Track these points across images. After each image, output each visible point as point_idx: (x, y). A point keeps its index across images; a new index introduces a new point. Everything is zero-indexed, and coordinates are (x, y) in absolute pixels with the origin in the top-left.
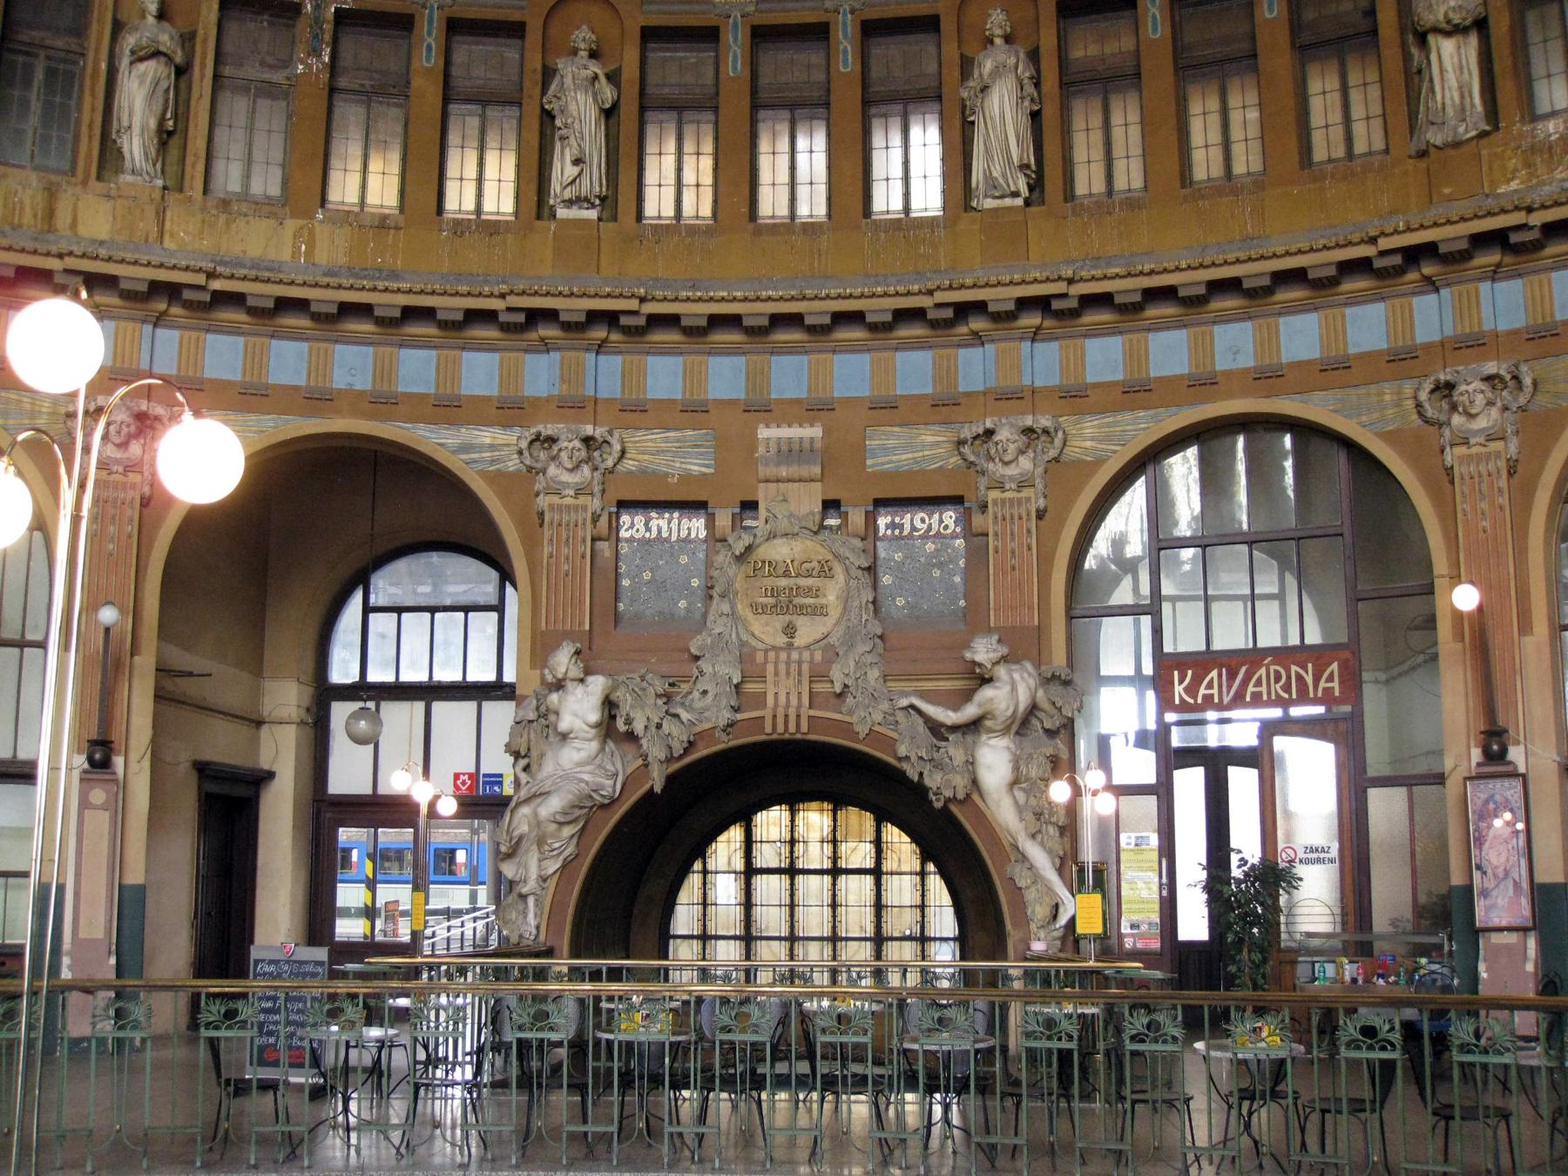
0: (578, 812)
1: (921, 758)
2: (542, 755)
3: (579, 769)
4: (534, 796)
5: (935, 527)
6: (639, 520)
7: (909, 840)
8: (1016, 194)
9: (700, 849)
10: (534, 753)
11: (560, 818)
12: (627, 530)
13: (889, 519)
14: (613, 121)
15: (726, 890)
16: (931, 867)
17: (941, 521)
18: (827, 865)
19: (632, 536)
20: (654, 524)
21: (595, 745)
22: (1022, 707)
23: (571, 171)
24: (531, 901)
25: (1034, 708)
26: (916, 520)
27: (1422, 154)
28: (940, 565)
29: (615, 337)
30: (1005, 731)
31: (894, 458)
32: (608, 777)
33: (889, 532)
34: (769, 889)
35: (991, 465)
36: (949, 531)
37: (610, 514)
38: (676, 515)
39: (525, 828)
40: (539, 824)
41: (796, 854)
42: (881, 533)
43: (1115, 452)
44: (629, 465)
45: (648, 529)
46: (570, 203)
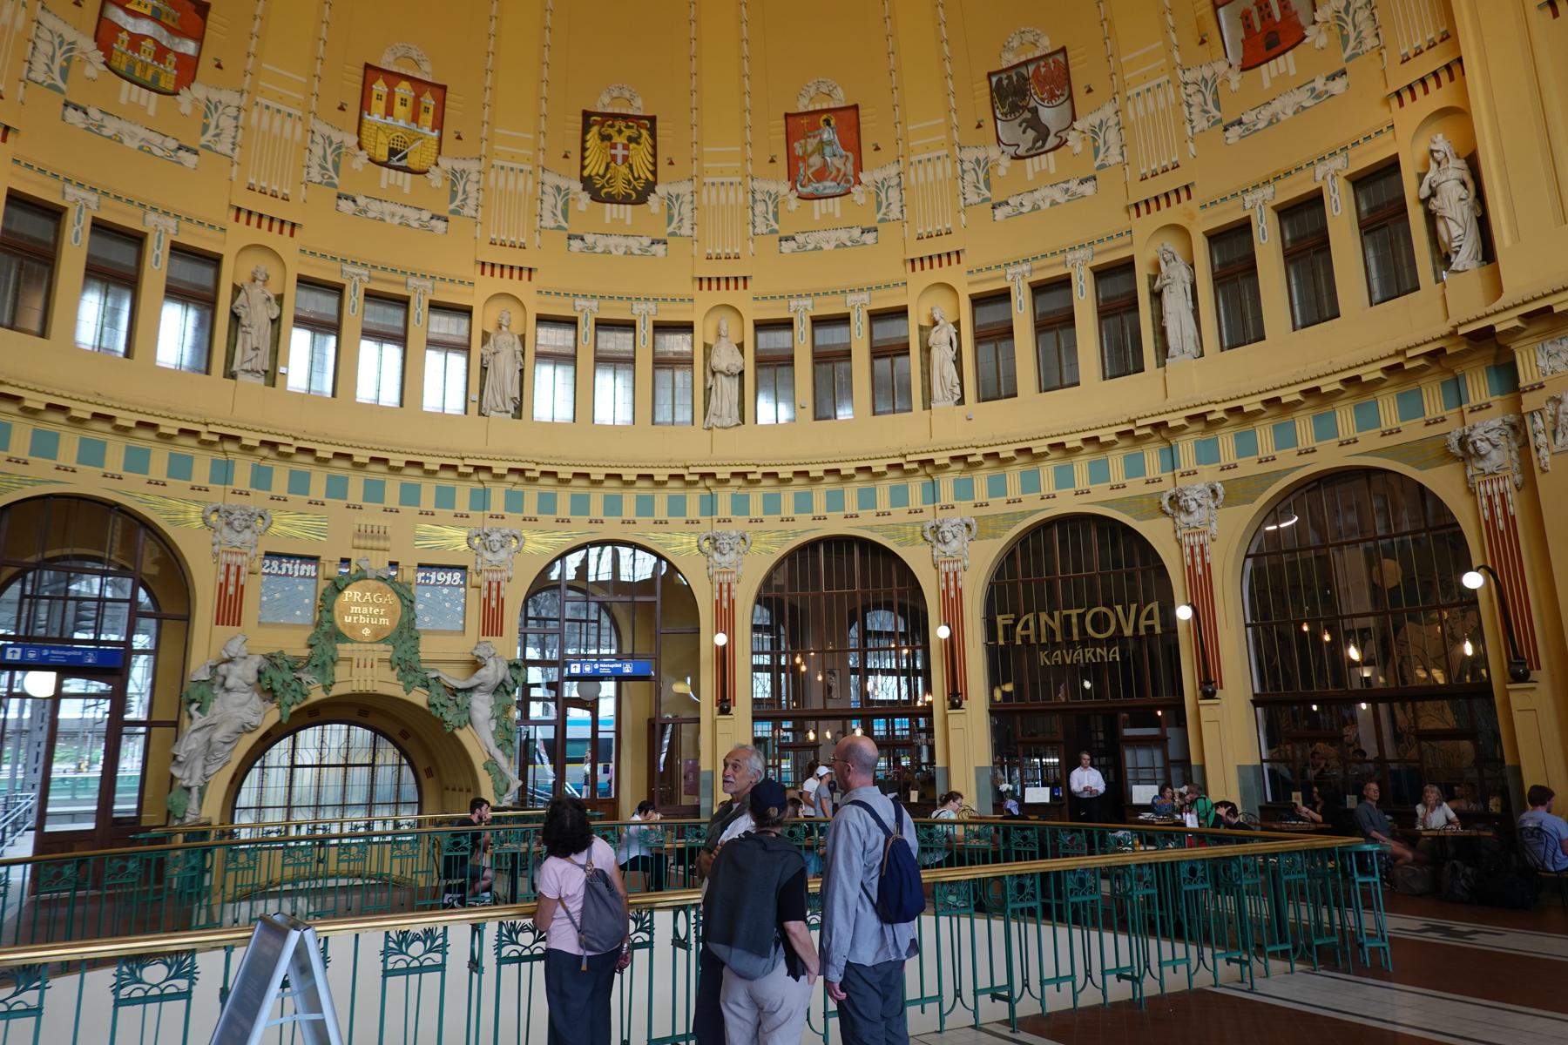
4: (205, 726)
6: (275, 563)
8: (508, 412)
14: (276, 326)
15: (277, 778)
18: (342, 762)
20: (284, 566)
22: (499, 681)
23: (251, 354)
24: (195, 791)
25: (504, 680)
26: (441, 576)
27: (709, 429)
28: (451, 602)
30: (488, 692)
34: (305, 778)
39: (193, 746)
40: (209, 742)
44: (272, 530)
46: (247, 371)
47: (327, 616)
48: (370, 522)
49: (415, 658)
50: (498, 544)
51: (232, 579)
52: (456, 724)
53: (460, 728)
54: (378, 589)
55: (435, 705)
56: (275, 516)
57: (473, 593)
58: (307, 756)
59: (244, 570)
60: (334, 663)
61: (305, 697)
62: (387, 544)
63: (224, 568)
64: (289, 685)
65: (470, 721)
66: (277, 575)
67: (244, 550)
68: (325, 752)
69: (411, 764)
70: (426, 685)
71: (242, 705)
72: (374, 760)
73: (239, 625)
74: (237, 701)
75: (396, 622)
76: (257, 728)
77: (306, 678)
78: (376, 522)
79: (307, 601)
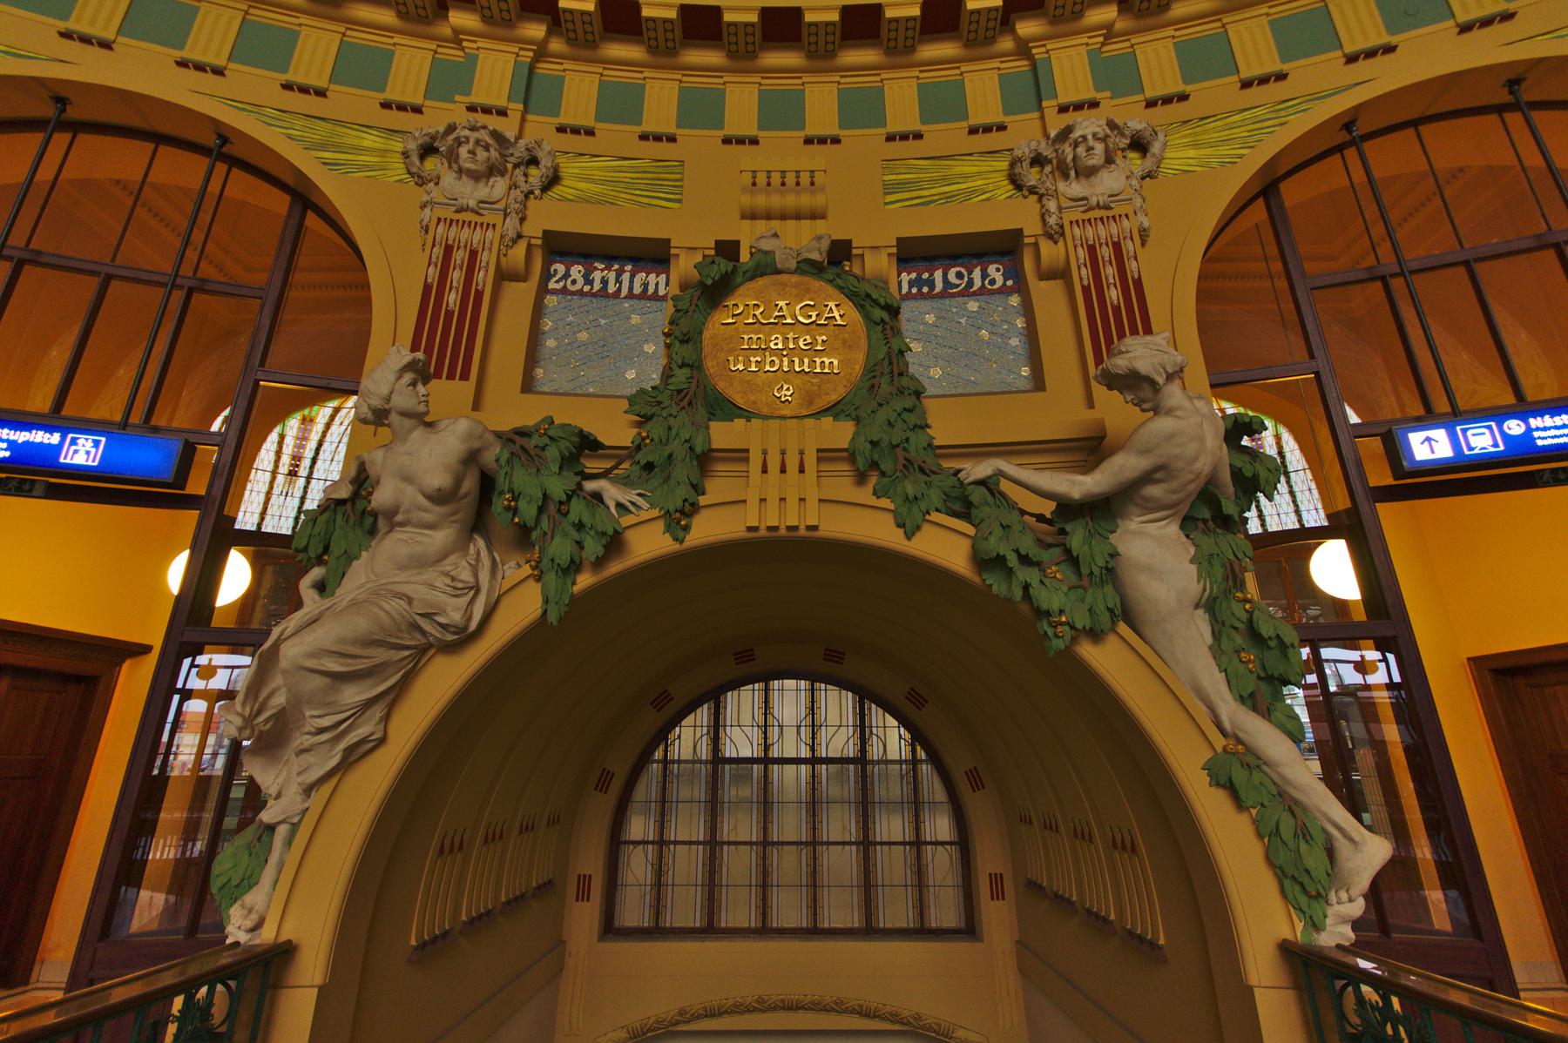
0: (382, 655)
1: (1025, 560)
2: (349, 558)
3: (402, 577)
5: (978, 283)
6: (577, 271)
7: (896, 724)
9: (662, 735)
10: (336, 550)
11: (334, 666)
12: (557, 282)
13: (914, 275)
16: (922, 754)
17: (984, 275)
19: (565, 286)
20: (597, 276)
21: (441, 537)
29: (556, 45)
31: (925, 193)
32: (457, 592)
33: (914, 290)
35: (1061, 186)
36: (999, 282)
37: (530, 246)
38: (628, 268)
41: (770, 741)
42: (905, 290)
43: (1240, 157)
45: (589, 281)
47: (683, 352)
48: (776, 164)
49: (918, 440)
50: (1099, 148)
51: (456, 276)
52: (1082, 621)
53: (1095, 635)
54: (804, 292)
55: (1000, 560)
56: (569, 168)
57: (1047, 296)
58: (741, 743)
59: (487, 258)
60: (705, 460)
61: (615, 543)
62: (819, 200)
63: (438, 251)
64: (563, 507)
65: (1126, 613)
66: (580, 293)
67: (489, 218)
68: (774, 733)
69: (935, 758)
70: (962, 505)
71: (422, 563)
72: (863, 750)
73: (465, 376)
74: (403, 551)
75: (858, 369)
76: (463, 639)
77: (612, 493)
78: (790, 164)
79: (649, 348)
